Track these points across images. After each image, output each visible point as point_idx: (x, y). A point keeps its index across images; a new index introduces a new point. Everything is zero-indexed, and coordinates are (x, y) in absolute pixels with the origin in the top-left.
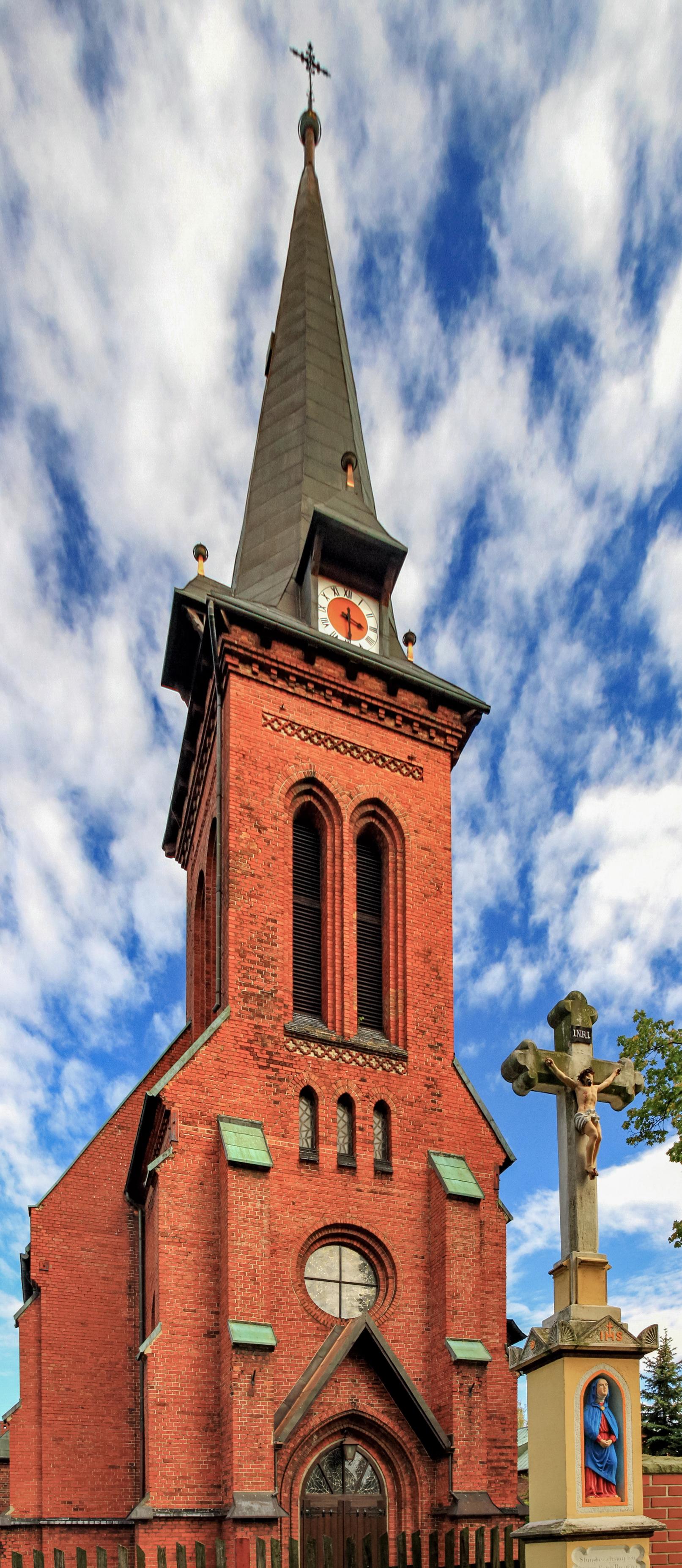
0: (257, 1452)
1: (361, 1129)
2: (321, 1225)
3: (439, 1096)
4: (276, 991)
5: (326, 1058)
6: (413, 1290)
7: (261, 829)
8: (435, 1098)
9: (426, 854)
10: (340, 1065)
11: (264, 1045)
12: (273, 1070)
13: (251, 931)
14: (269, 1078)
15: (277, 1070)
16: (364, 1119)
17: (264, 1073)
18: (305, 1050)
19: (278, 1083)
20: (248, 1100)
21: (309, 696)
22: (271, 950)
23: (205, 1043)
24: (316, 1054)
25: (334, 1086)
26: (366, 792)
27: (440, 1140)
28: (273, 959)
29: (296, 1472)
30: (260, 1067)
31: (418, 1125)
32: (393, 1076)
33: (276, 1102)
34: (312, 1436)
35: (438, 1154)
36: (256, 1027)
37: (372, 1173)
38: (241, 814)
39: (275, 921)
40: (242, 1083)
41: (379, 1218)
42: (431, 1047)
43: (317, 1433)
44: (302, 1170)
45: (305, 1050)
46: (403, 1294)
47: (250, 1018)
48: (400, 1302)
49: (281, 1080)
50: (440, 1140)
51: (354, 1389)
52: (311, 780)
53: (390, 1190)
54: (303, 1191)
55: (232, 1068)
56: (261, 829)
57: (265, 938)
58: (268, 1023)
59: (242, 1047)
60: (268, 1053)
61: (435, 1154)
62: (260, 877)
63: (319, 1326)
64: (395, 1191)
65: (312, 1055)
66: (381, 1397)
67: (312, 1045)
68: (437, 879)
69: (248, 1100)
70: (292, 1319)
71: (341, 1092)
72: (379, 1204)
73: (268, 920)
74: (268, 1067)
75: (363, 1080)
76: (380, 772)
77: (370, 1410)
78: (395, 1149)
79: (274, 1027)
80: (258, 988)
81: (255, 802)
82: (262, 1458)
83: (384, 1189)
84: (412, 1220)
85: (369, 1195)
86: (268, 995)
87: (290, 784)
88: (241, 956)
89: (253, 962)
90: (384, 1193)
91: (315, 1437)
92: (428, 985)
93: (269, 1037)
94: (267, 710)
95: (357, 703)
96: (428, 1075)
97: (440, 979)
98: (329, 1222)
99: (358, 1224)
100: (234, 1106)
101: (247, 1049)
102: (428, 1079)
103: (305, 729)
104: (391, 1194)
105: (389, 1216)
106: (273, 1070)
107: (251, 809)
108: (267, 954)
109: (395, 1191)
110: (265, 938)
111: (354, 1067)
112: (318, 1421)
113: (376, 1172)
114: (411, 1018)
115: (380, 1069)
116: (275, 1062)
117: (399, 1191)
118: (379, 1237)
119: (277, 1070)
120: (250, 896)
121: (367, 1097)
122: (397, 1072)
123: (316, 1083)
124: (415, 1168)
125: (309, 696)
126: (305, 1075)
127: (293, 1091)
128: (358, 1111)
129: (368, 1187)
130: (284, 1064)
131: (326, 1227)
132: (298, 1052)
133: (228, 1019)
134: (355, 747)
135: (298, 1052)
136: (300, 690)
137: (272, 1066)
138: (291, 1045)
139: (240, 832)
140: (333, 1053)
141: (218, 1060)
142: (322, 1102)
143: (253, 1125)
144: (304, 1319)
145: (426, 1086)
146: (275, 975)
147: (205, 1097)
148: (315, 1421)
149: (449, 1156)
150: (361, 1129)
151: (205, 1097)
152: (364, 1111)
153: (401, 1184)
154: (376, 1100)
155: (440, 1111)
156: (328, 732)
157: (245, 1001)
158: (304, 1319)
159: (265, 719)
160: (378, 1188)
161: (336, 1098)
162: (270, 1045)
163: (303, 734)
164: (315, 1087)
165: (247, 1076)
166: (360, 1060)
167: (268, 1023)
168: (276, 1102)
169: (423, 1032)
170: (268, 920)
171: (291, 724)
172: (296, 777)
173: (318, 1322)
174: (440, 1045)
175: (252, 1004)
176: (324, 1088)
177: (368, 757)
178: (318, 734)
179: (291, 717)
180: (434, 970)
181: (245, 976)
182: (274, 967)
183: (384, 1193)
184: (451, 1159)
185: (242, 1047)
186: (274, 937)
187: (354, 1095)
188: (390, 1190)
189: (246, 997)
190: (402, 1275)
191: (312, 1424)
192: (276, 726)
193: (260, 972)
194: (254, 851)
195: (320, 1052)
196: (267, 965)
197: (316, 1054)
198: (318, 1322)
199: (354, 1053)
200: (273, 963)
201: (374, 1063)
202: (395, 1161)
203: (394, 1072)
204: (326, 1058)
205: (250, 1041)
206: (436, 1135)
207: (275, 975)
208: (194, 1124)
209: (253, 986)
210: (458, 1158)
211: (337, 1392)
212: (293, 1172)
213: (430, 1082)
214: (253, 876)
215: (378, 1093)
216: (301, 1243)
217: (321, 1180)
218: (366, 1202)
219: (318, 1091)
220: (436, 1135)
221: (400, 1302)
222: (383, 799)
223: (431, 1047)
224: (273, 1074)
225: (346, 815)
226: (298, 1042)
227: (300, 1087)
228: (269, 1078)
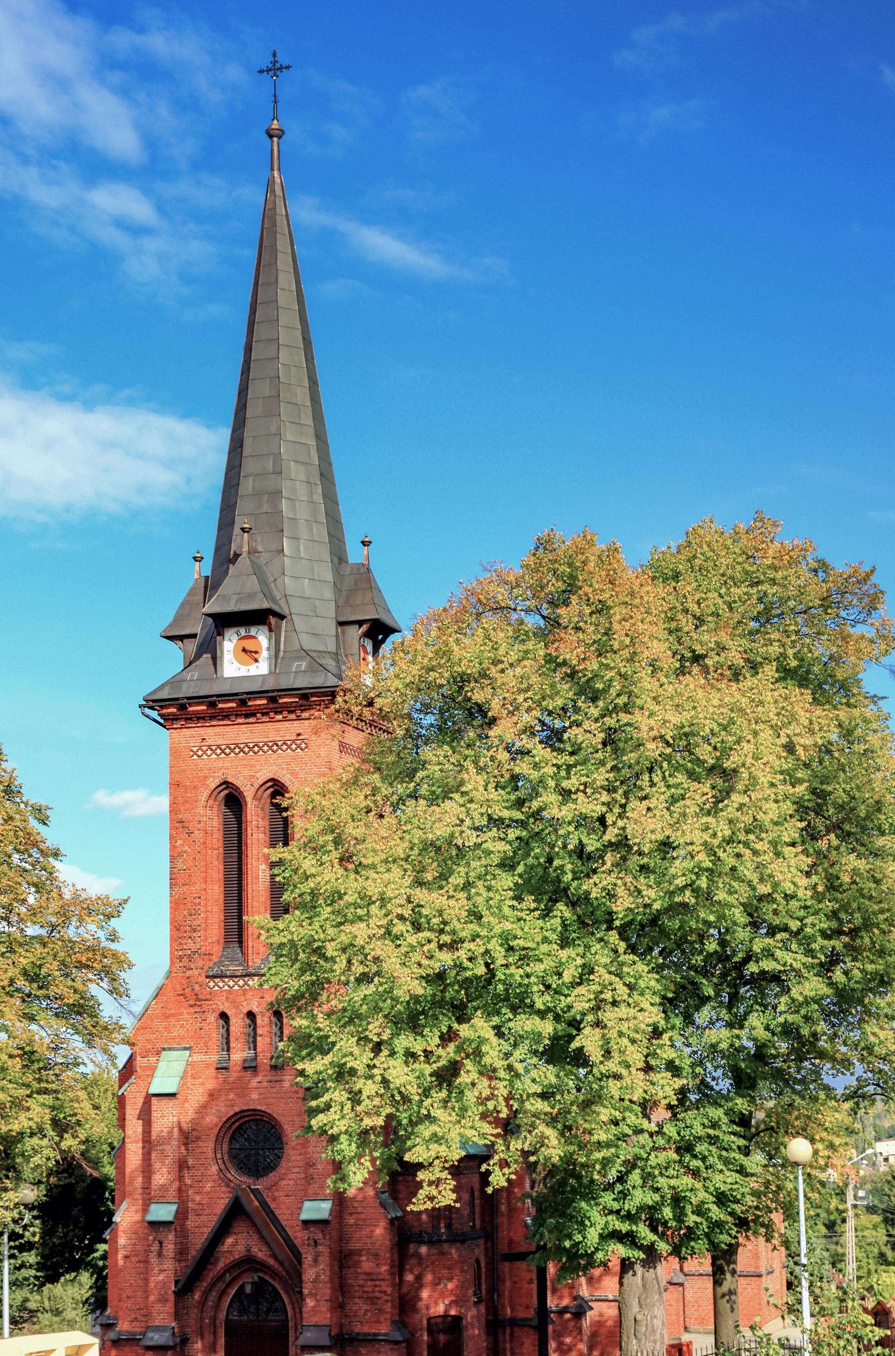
2: (232, 1113)
5: (236, 988)
7: (189, 834)
45: (221, 984)
52: (226, 783)
60: (196, 995)
71: (245, 1011)
75: (262, 998)
98: (237, 1109)
103: (218, 746)
116: (200, 1000)
127: (212, 1018)
128: (259, 1021)
131: (236, 1114)
138: (212, 984)
140: (241, 983)
142: (233, 1021)
143: (186, 1049)
163: (219, 751)
172: (213, 786)
179: (209, 742)
191: (218, 1268)
192: (200, 753)
195: (231, 983)
204: (236, 988)
216: (217, 1129)
219: (229, 1013)
225: (249, 800)
227: (216, 1014)
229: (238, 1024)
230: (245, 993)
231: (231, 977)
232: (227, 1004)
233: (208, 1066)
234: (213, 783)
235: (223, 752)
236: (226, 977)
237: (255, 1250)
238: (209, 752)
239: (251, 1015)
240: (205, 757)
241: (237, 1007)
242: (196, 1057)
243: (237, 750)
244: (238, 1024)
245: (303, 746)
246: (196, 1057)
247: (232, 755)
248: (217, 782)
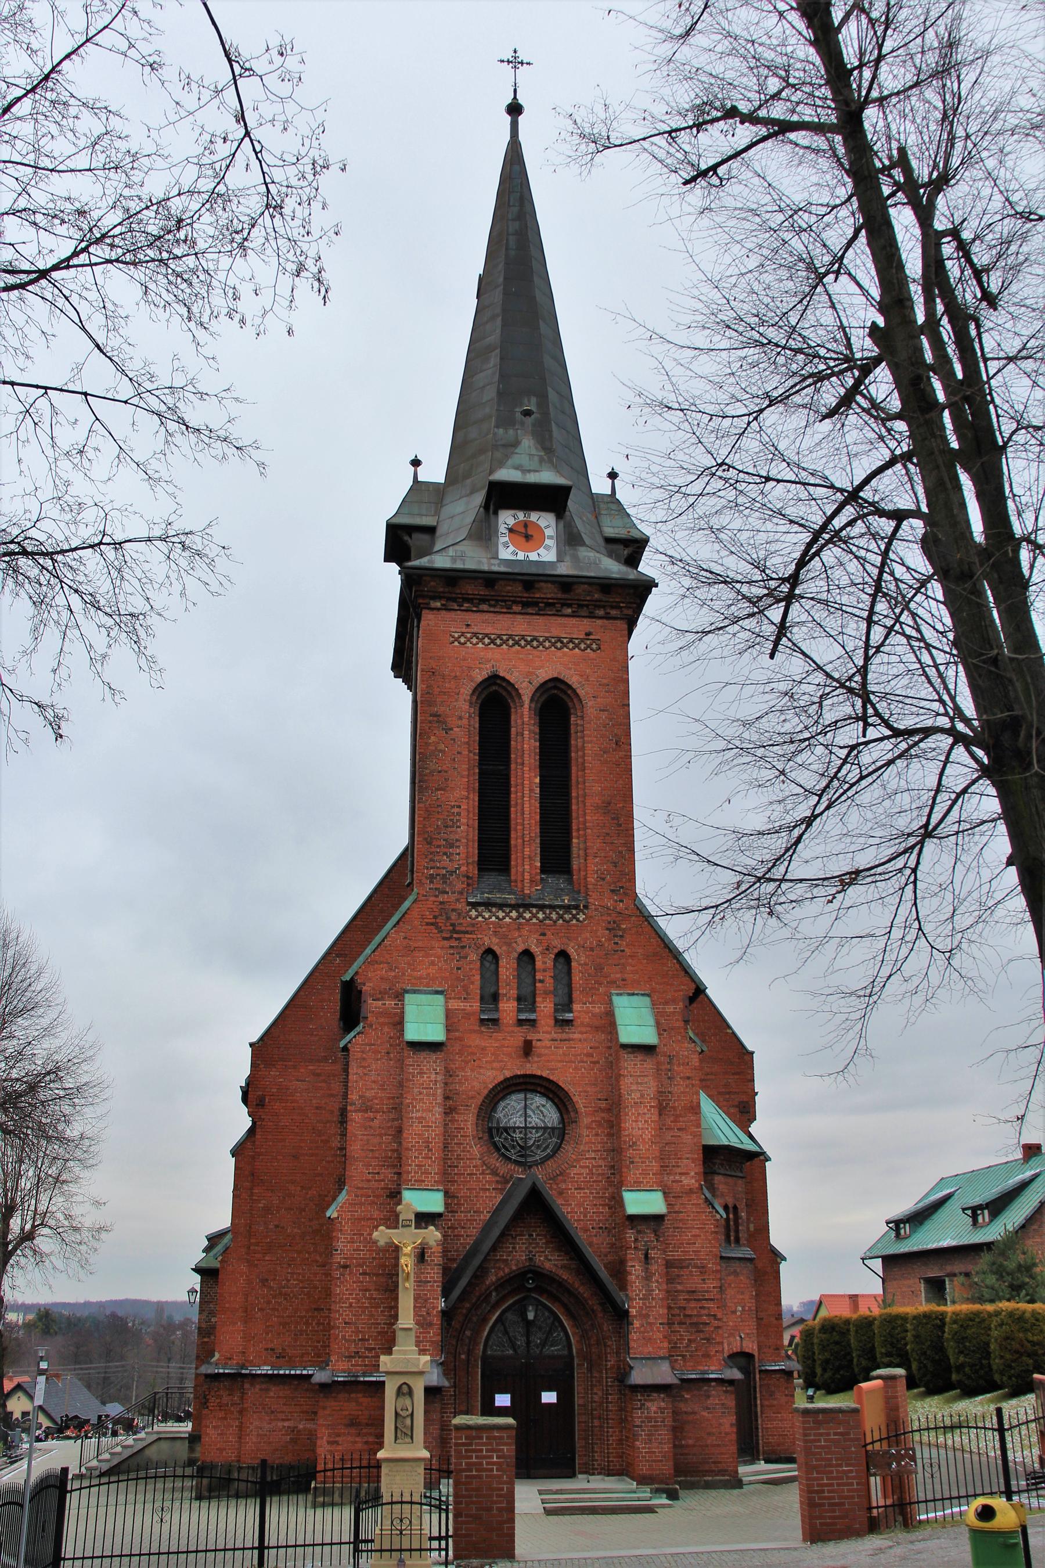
0: (425, 1319)
1: (541, 981)
3: (621, 936)
4: (459, 869)
5: (507, 919)
6: (597, 1135)
8: (616, 940)
9: (604, 716)
10: (520, 924)
11: (448, 918)
12: (456, 939)
13: (438, 819)
14: (452, 947)
15: (459, 939)
16: (544, 970)
17: (446, 943)
18: (487, 915)
19: (460, 950)
20: (432, 970)
21: (492, 609)
22: (456, 833)
23: (394, 926)
24: (497, 918)
25: (514, 945)
26: (544, 674)
27: (623, 980)
28: (457, 840)
29: (477, 1332)
30: (445, 939)
31: (599, 968)
32: (574, 925)
33: (458, 969)
34: (491, 1293)
35: (621, 994)
36: (441, 903)
37: (552, 1022)
38: (430, 722)
39: (459, 807)
40: (427, 956)
41: (560, 1065)
42: (612, 891)
43: (496, 1289)
44: (483, 1029)
45: (487, 915)
46: (585, 1139)
47: (437, 896)
48: (582, 1147)
49: (463, 947)
50: (623, 980)
51: (530, 1244)
53: (571, 1036)
54: (483, 1049)
55: (420, 944)
56: (448, 730)
57: (451, 823)
58: (452, 897)
59: (427, 924)
60: (453, 925)
61: (618, 994)
62: (446, 772)
63: (498, 1178)
64: (576, 1036)
65: (494, 919)
66: (560, 1250)
67: (494, 910)
68: (616, 735)
69: (432, 970)
70: (472, 1174)
71: (520, 948)
72: (561, 1051)
73: (453, 807)
74: (451, 937)
75: (544, 934)
76: (559, 653)
77: (548, 1265)
78: (576, 994)
79: (458, 900)
80: (444, 868)
81: (443, 708)
82: (431, 1325)
83: (564, 1036)
84: (594, 1063)
85: (548, 1043)
86: (451, 873)
87: (474, 685)
88: (428, 843)
89: (439, 846)
90: (565, 1040)
91: (494, 1294)
92: (608, 834)
93: (453, 910)
94: (452, 629)
95: (535, 604)
96: (609, 919)
97: (620, 825)
98: (508, 1074)
99: (539, 1073)
100: (421, 978)
101: (432, 924)
102: (609, 923)
103: (487, 635)
104: (573, 1040)
105: (571, 1062)
106: (456, 939)
107: (439, 716)
108: (452, 836)
109: (576, 1036)
110: (451, 823)
111: (534, 924)
112: (494, 1279)
113: (557, 1021)
114: (592, 867)
115: (561, 921)
116: (457, 932)
117: (580, 1036)
118: (560, 1084)
119: (459, 939)
120: (438, 789)
121: (547, 949)
122: (578, 920)
123: (497, 944)
124: (597, 1010)
125: (492, 609)
126: (486, 939)
127: (474, 957)
128: (539, 964)
129: (548, 1036)
130: (467, 932)
132: (480, 919)
133: (415, 901)
134: (535, 639)
135: (480, 919)
136: (484, 607)
137: (455, 936)
138: (473, 913)
139: (429, 738)
140: (514, 914)
141: (405, 938)
142: (503, 962)
143: (437, 992)
144: (483, 1173)
145: (607, 929)
146: (459, 854)
147: (393, 974)
148: (492, 1278)
149: (633, 994)
150: (541, 981)
151: (393, 974)
152: (545, 963)
153: (584, 1029)
154: (556, 951)
155: (623, 951)
156: (510, 633)
157: (431, 882)
158: (483, 1173)
159: (453, 637)
160: (559, 1036)
161: (516, 955)
162: (453, 917)
163: (487, 641)
164: (495, 948)
165: (433, 948)
166: (541, 915)
167: (452, 897)
168: (458, 969)
169: (603, 879)
170: (453, 807)
171: (475, 634)
173: (497, 1175)
174: (622, 887)
175: (438, 884)
176: (504, 948)
177: (547, 644)
178: (499, 636)
179: (475, 630)
180: (613, 819)
181: (432, 860)
182: (458, 847)
183: (565, 1040)
184: (635, 997)
185: (427, 924)
186: (458, 820)
187: (535, 949)
188: (571, 1036)
189: (432, 878)
190: (586, 1120)
192: (462, 640)
193: (445, 854)
194: (440, 751)
195: (501, 914)
196: (452, 846)
197: (497, 918)
198: (497, 1175)
199: (534, 910)
200: (458, 844)
201: (554, 916)
202: (576, 1007)
203: (574, 922)
204: (507, 919)
205: (435, 917)
206: (618, 976)
207: (459, 854)
208: (382, 999)
209: (438, 868)
210: (643, 995)
211: (514, 1248)
212: (475, 1031)
213: (612, 926)
214: (440, 772)
215: (557, 944)
216: (480, 1099)
217: (500, 1036)
218: (546, 1051)
220: (618, 976)
221: (582, 1147)
222: (562, 677)
223: (612, 891)
224: (455, 944)
225: (526, 699)
226: (480, 909)
228: (452, 947)
229: (507, 968)
230: (519, 928)
231: (501, 906)
232: (495, 940)
233: (467, 1015)
234: (480, 676)
235: (493, 642)
236: (494, 905)
237: (540, 1259)
238: (474, 640)
239: (527, 955)
240: (469, 644)
241: (509, 945)
242: (454, 1004)
243: (511, 642)
244: (507, 968)
245: (594, 646)
246: (454, 1004)
247: (504, 646)
248: (485, 674)
